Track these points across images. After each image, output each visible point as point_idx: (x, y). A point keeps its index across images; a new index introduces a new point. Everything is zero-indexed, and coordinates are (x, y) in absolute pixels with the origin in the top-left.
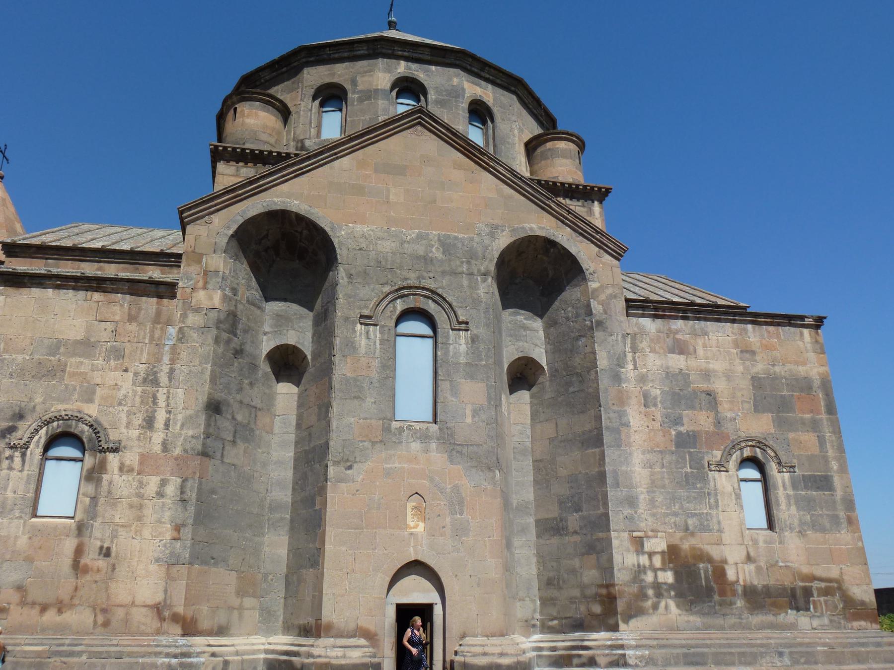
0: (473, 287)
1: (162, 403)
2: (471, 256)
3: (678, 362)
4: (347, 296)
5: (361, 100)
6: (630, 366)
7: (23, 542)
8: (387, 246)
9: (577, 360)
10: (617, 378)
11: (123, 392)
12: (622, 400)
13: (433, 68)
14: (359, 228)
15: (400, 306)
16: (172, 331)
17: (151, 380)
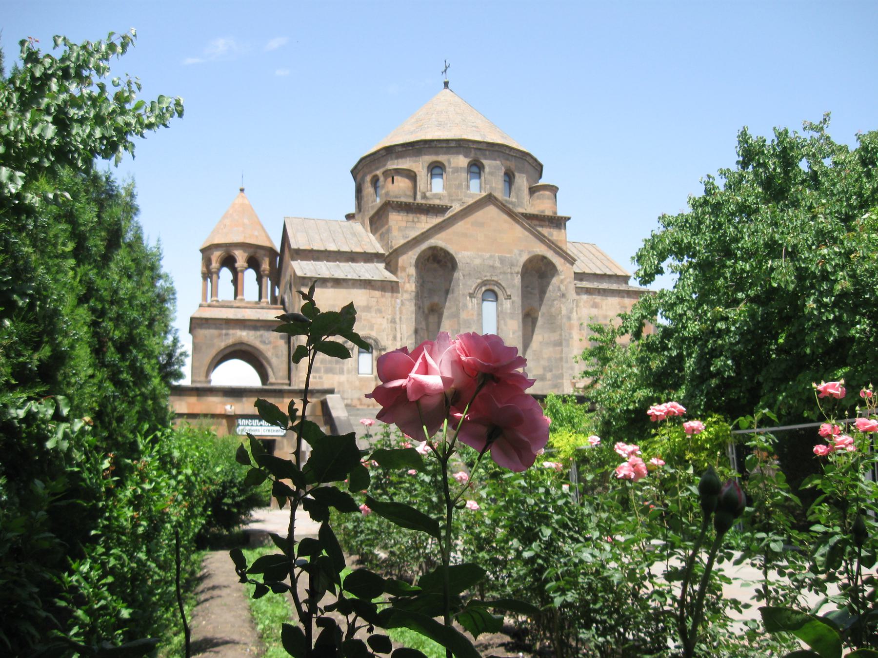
0: (513, 279)
1: (398, 330)
2: (512, 265)
3: (594, 312)
4: (463, 284)
5: (453, 172)
6: (575, 314)
7: (357, 383)
8: (477, 262)
9: (553, 310)
10: (569, 318)
11: (383, 327)
12: (571, 327)
13: (487, 153)
14: (466, 254)
15: (484, 289)
16: (399, 301)
17: (393, 321)
